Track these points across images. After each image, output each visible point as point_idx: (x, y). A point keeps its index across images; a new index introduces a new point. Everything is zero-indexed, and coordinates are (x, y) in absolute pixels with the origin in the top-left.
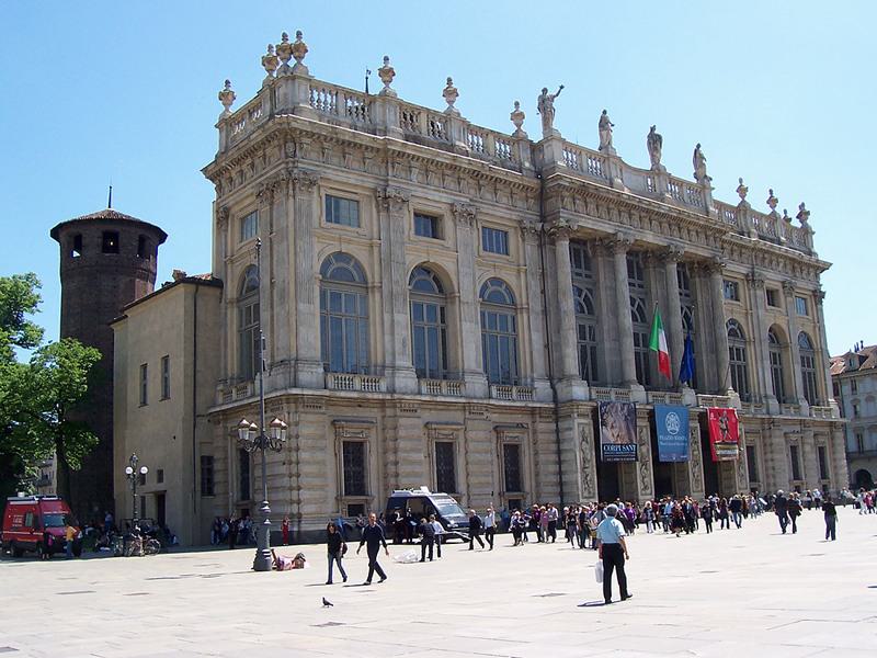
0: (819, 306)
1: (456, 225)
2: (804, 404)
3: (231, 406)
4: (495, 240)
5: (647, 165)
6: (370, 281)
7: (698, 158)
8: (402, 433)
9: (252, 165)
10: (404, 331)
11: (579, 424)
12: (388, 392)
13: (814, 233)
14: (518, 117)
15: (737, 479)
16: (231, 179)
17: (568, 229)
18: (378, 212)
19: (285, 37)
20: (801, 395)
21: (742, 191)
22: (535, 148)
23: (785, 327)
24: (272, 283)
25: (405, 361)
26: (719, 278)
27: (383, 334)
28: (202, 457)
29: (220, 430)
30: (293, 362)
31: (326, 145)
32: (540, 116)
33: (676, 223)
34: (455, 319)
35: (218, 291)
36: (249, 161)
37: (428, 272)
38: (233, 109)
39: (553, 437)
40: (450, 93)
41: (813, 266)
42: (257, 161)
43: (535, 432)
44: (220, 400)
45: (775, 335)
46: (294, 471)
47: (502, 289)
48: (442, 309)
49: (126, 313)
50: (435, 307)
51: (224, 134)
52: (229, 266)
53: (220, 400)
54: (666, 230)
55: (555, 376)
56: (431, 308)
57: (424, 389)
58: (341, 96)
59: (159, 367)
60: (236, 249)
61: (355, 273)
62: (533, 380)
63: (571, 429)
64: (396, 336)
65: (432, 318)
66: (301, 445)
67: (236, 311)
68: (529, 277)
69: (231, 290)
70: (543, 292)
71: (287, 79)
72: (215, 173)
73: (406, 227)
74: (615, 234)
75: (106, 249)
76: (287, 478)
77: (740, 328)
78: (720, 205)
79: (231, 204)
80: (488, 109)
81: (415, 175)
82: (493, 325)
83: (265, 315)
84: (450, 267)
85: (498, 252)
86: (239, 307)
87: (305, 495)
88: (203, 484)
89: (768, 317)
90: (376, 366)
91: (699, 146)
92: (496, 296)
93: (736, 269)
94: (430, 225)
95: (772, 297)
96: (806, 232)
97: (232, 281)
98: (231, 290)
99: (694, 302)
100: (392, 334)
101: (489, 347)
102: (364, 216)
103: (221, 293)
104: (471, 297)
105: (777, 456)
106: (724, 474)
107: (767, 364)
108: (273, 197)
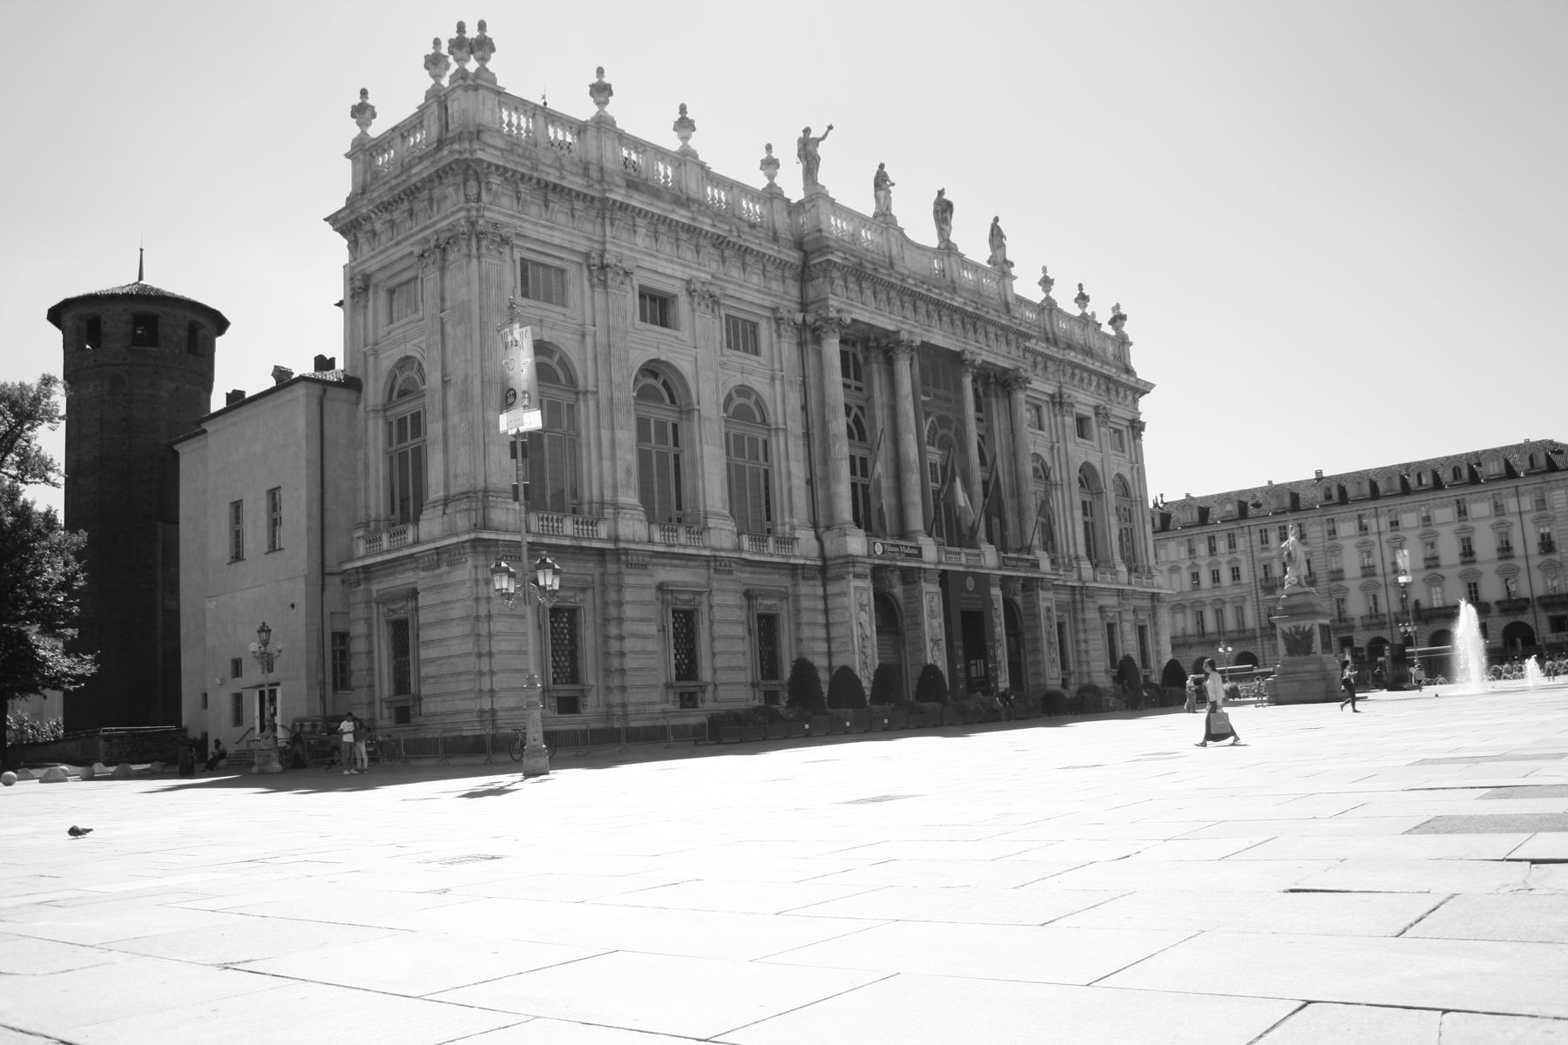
1: (693, 310)
2: (1122, 568)
3: (379, 559)
4: (742, 335)
6: (581, 382)
7: (996, 236)
8: (628, 595)
9: (411, 213)
10: (628, 456)
11: (856, 588)
12: (609, 540)
14: (770, 164)
15: (1047, 665)
16: (374, 234)
18: (592, 286)
19: (461, 27)
20: (1117, 558)
22: (794, 209)
23: (1098, 466)
24: (444, 383)
25: (630, 498)
26: (1021, 396)
27: (600, 458)
28: (334, 635)
29: (359, 594)
30: (481, 495)
31: (522, 188)
32: (800, 167)
33: (971, 321)
34: (692, 440)
35: (352, 395)
36: (405, 206)
37: (656, 375)
38: (376, 130)
39: (820, 605)
40: (684, 124)
41: (1132, 388)
42: (417, 206)
43: (797, 597)
44: (361, 551)
45: (1088, 477)
46: (485, 650)
47: (751, 403)
48: (675, 427)
49: (204, 426)
51: (360, 167)
52: (371, 360)
53: (361, 551)
54: (959, 330)
55: (821, 522)
56: (661, 426)
57: (657, 537)
58: (540, 119)
59: (264, 504)
60: (381, 333)
61: (560, 372)
62: (793, 528)
63: (844, 594)
64: (619, 462)
65: (661, 438)
66: (494, 611)
67: (381, 423)
68: (787, 388)
69: (374, 393)
70: (804, 408)
71: (466, 88)
72: (348, 223)
73: (630, 308)
74: (896, 333)
75: (136, 340)
76: (472, 659)
78: (1021, 300)
79: (373, 268)
80: (732, 154)
81: (641, 240)
82: (740, 451)
83: (433, 429)
84: (686, 367)
85: (746, 350)
86: (385, 418)
87: (500, 682)
88: (335, 673)
89: (1080, 452)
90: (591, 502)
91: (996, 219)
92: (744, 409)
93: (1042, 386)
94: (658, 307)
95: (1081, 422)
96: (1123, 342)
97: (376, 380)
98: (374, 393)
99: (990, 429)
100: (613, 458)
101: (735, 477)
102: (573, 292)
103: (358, 398)
104: (714, 412)
106: (1030, 658)
107: (1078, 513)
108: (444, 259)
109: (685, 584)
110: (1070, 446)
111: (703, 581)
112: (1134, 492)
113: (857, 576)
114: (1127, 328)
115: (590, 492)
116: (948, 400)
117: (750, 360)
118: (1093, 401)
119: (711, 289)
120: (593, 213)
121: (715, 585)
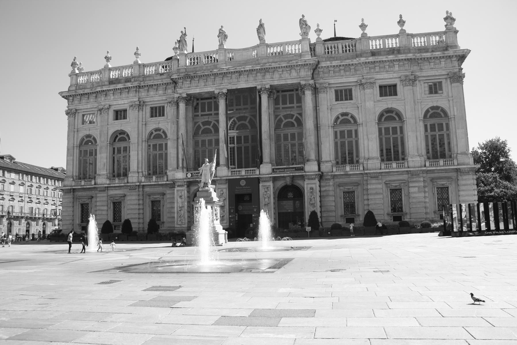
0: (454, 85)
5: (258, 42)
7: (303, 24)
8: (98, 200)
11: (178, 190)
12: (95, 184)
13: (456, 32)
17: (183, 98)
21: (363, 26)
50: (126, 147)
61: (93, 141)
77: (352, 117)
85: (160, 116)
91: (303, 16)
94: (120, 115)
105: (370, 197)
109: (116, 194)
110: (370, 104)
111: (126, 193)
112: (450, 114)
113: (178, 186)
114: (456, 25)
115: (97, 172)
116: (245, 109)
117: (161, 118)
118: (395, 75)
119: (136, 103)
120: (100, 95)
121: (128, 194)
